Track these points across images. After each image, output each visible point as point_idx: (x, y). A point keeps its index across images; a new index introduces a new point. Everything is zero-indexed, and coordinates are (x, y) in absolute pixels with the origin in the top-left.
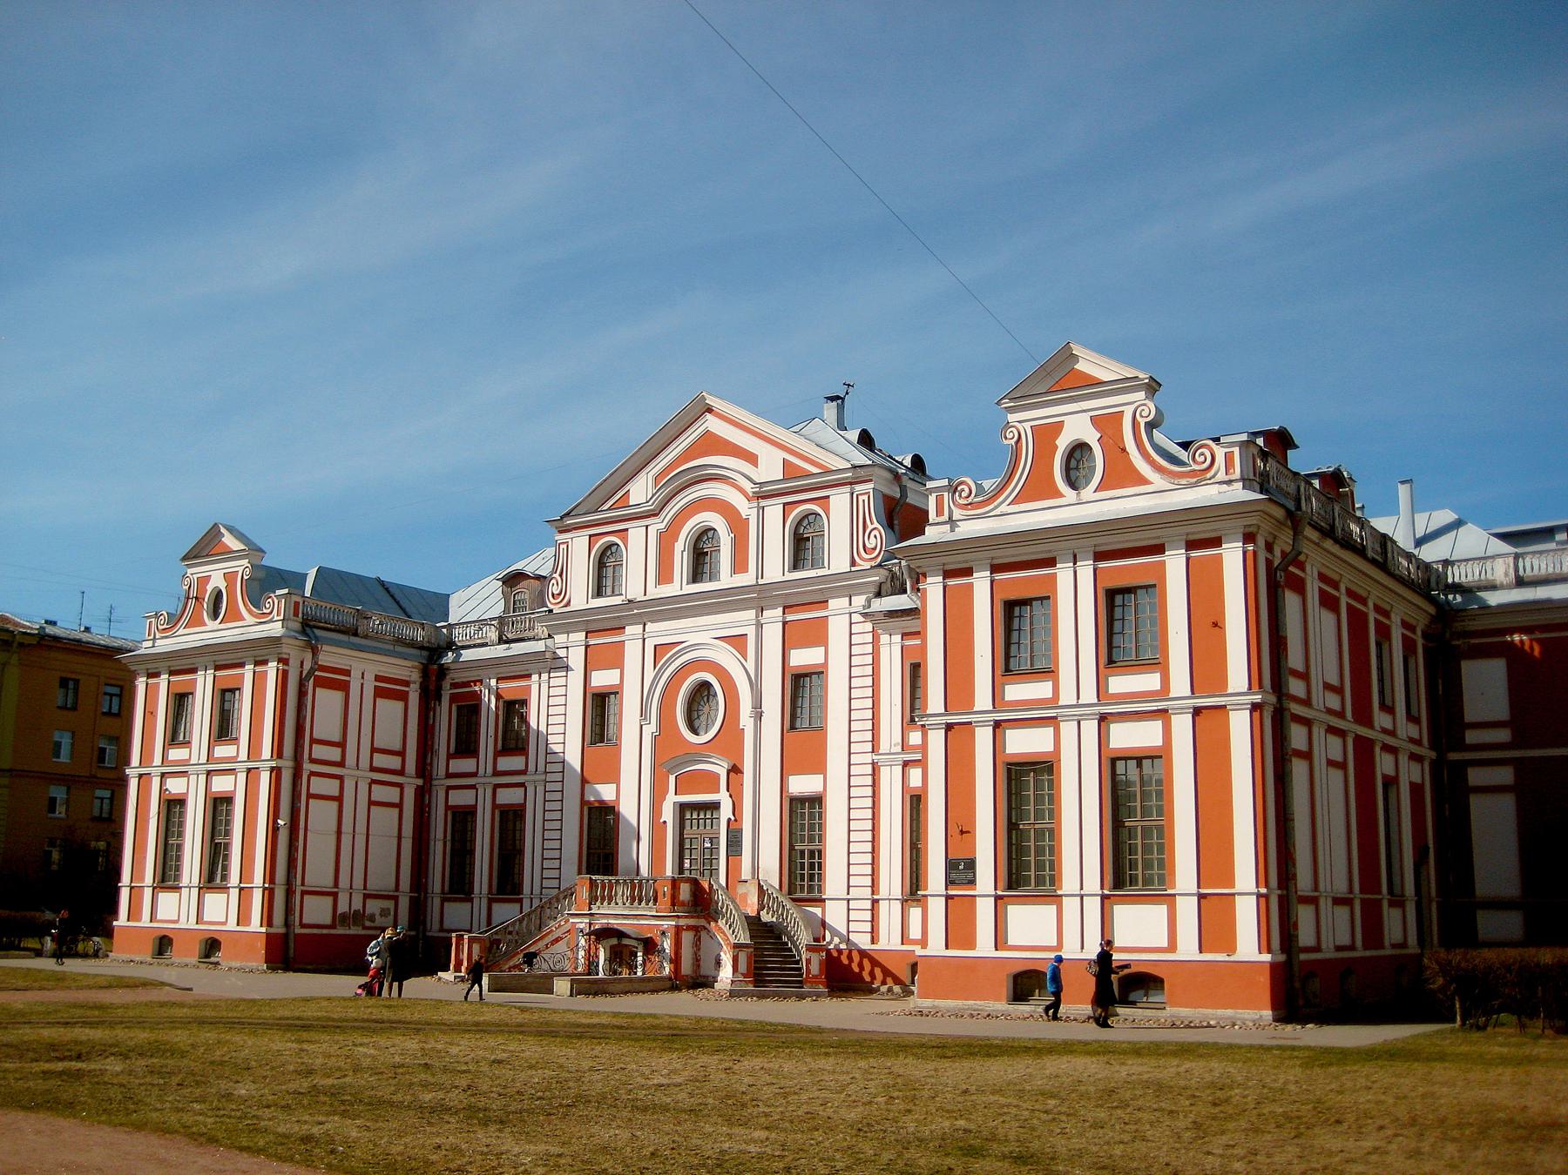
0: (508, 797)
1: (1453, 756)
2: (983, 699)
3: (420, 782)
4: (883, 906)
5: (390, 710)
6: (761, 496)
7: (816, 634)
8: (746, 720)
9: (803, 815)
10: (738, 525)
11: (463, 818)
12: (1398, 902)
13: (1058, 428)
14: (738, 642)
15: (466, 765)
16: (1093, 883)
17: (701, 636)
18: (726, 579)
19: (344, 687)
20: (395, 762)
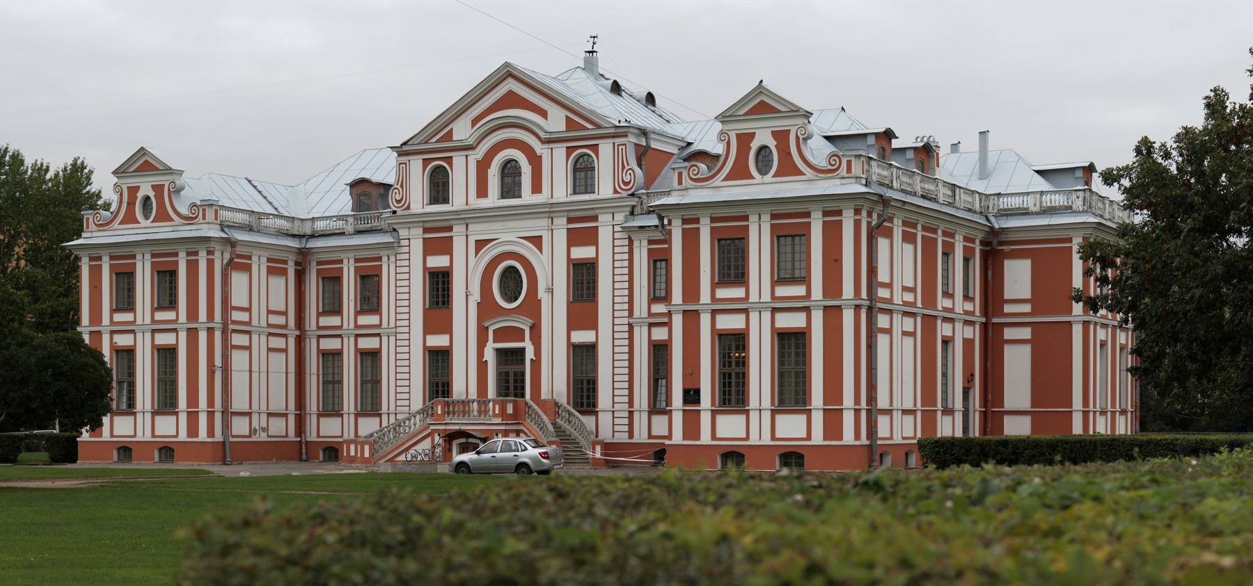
0: (366, 343)
1: (995, 320)
2: (705, 297)
3: (298, 333)
4: (636, 416)
5: (278, 283)
6: (549, 141)
7: (590, 237)
8: (542, 294)
9: (584, 356)
10: (536, 161)
11: (331, 358)
12: (948, 411)
13: (752, 136)
14: (537, 241)
15: (334, 321)
16: (767, 403)
17: (508, 236)
18: (527, 197)
19: (247, 268)
20: (280, 320)
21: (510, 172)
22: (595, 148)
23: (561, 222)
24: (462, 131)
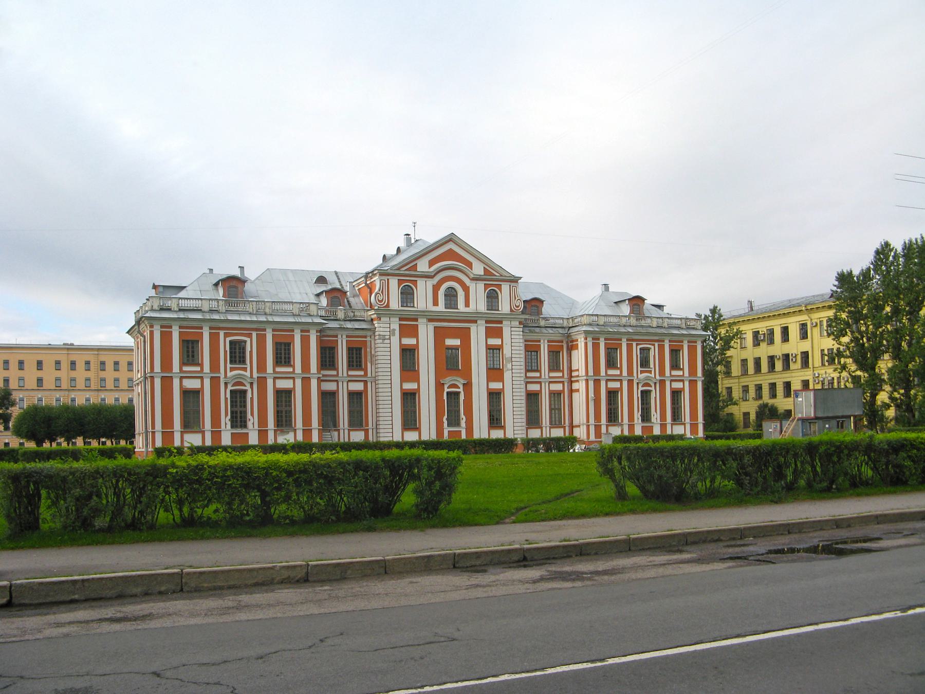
7: (498, 333)
9: (495, 397)
10: (466, 289)
21: (451, 295)
22: (499, 287)
23: (482, 322)
24: (423, 266)
